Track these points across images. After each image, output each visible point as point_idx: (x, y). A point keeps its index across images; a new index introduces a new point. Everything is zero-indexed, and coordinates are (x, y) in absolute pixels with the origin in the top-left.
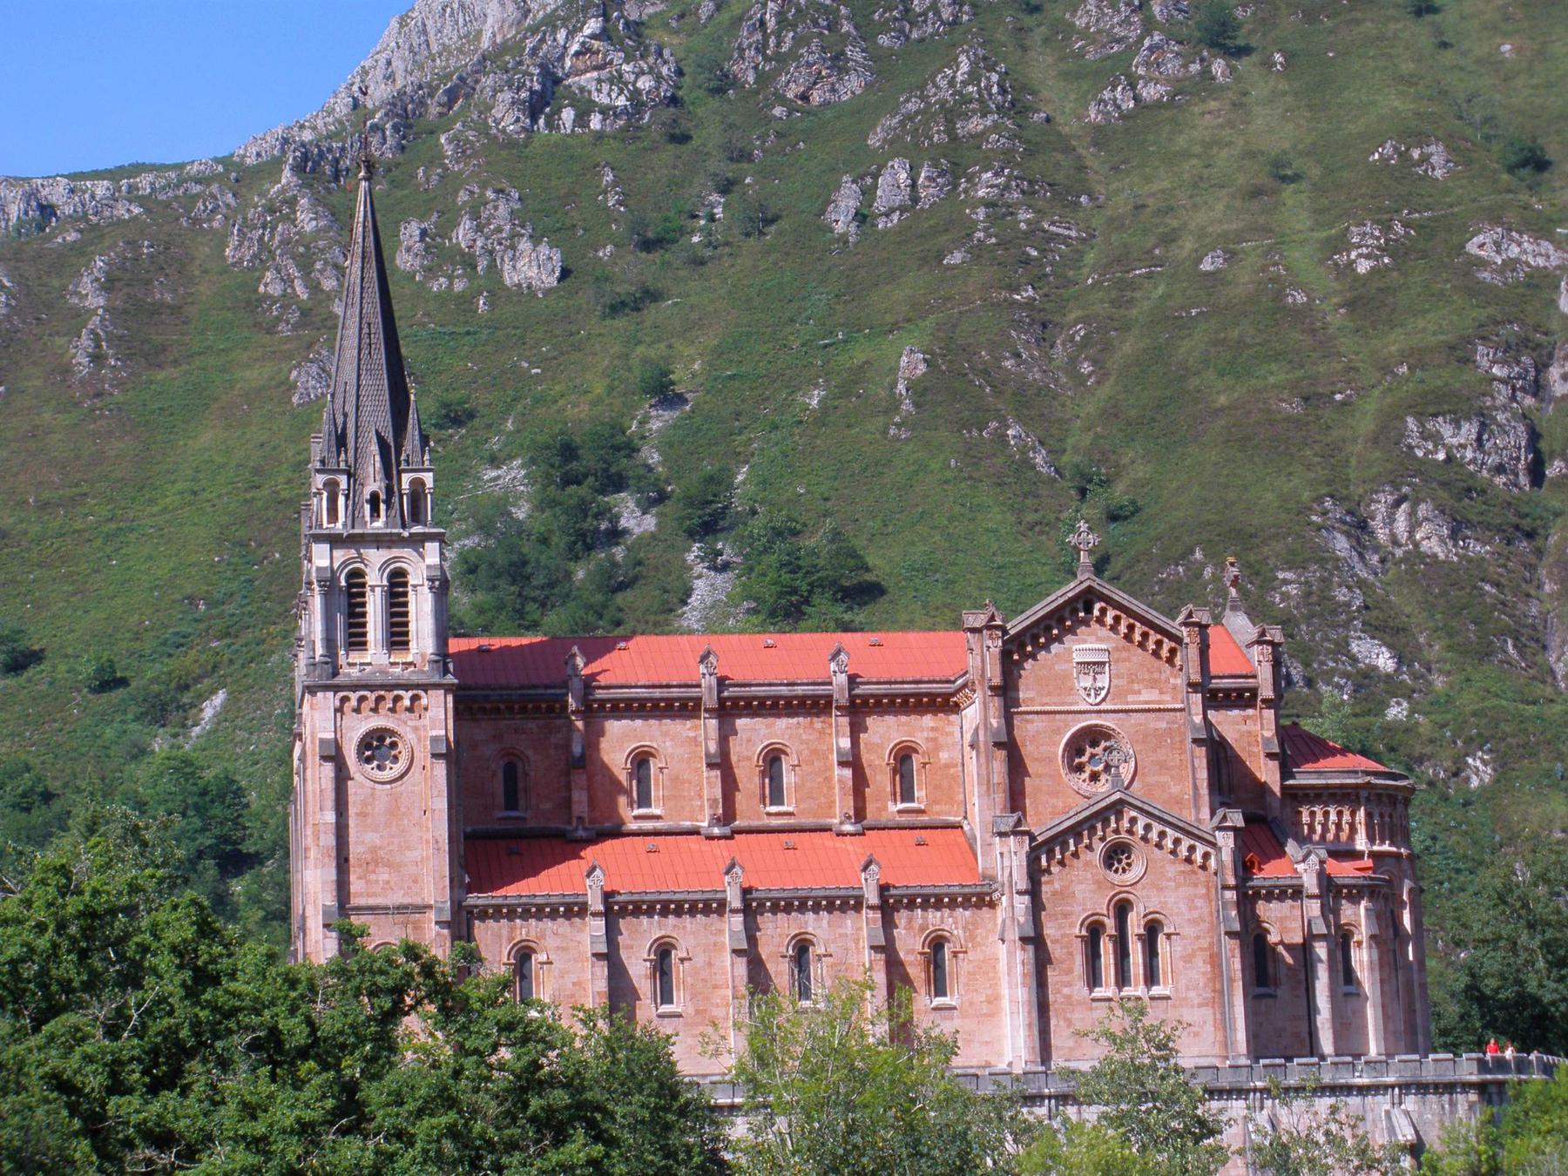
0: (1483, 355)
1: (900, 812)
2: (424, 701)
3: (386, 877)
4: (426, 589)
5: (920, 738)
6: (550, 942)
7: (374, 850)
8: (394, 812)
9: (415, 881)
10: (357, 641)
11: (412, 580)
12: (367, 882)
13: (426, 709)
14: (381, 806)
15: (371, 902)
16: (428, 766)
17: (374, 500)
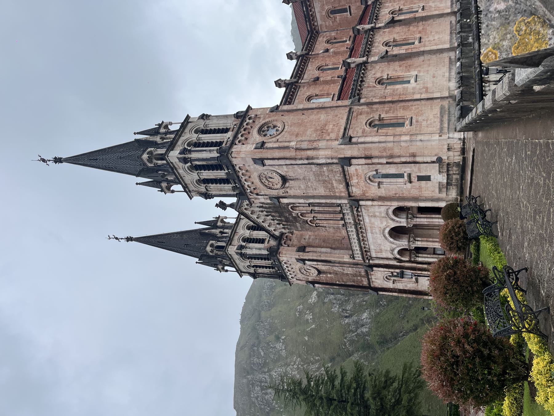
0: (326, 301)
1: (349, 40)
2: (253, 115)
3: (331, 126)
4: (208, 121)
5: (325, 39)
6: (378, 75)
7: (316, 130)
8: (300, 125)
9: (337, 116)
10: (218, 144)
11: (202, 127)
12: (331, 132)
13: (256, 115)
14: (296, 129)
15: (342, 130)
16: (282, 113)
17: (162, 139)
